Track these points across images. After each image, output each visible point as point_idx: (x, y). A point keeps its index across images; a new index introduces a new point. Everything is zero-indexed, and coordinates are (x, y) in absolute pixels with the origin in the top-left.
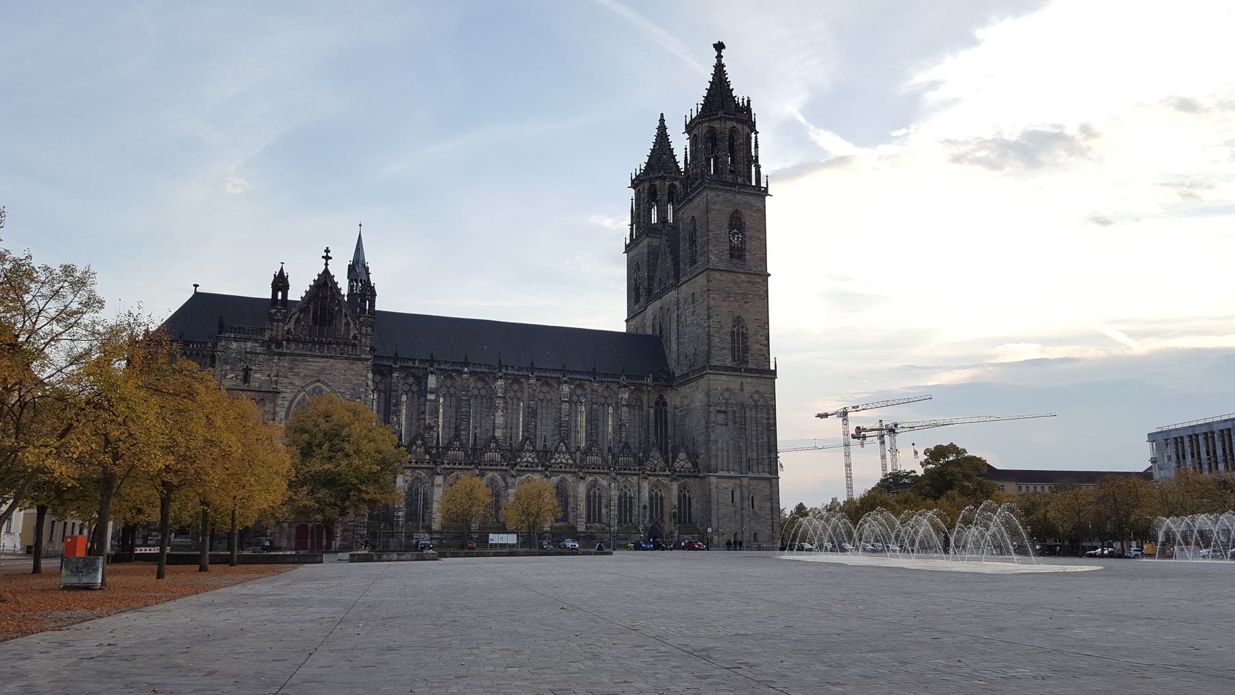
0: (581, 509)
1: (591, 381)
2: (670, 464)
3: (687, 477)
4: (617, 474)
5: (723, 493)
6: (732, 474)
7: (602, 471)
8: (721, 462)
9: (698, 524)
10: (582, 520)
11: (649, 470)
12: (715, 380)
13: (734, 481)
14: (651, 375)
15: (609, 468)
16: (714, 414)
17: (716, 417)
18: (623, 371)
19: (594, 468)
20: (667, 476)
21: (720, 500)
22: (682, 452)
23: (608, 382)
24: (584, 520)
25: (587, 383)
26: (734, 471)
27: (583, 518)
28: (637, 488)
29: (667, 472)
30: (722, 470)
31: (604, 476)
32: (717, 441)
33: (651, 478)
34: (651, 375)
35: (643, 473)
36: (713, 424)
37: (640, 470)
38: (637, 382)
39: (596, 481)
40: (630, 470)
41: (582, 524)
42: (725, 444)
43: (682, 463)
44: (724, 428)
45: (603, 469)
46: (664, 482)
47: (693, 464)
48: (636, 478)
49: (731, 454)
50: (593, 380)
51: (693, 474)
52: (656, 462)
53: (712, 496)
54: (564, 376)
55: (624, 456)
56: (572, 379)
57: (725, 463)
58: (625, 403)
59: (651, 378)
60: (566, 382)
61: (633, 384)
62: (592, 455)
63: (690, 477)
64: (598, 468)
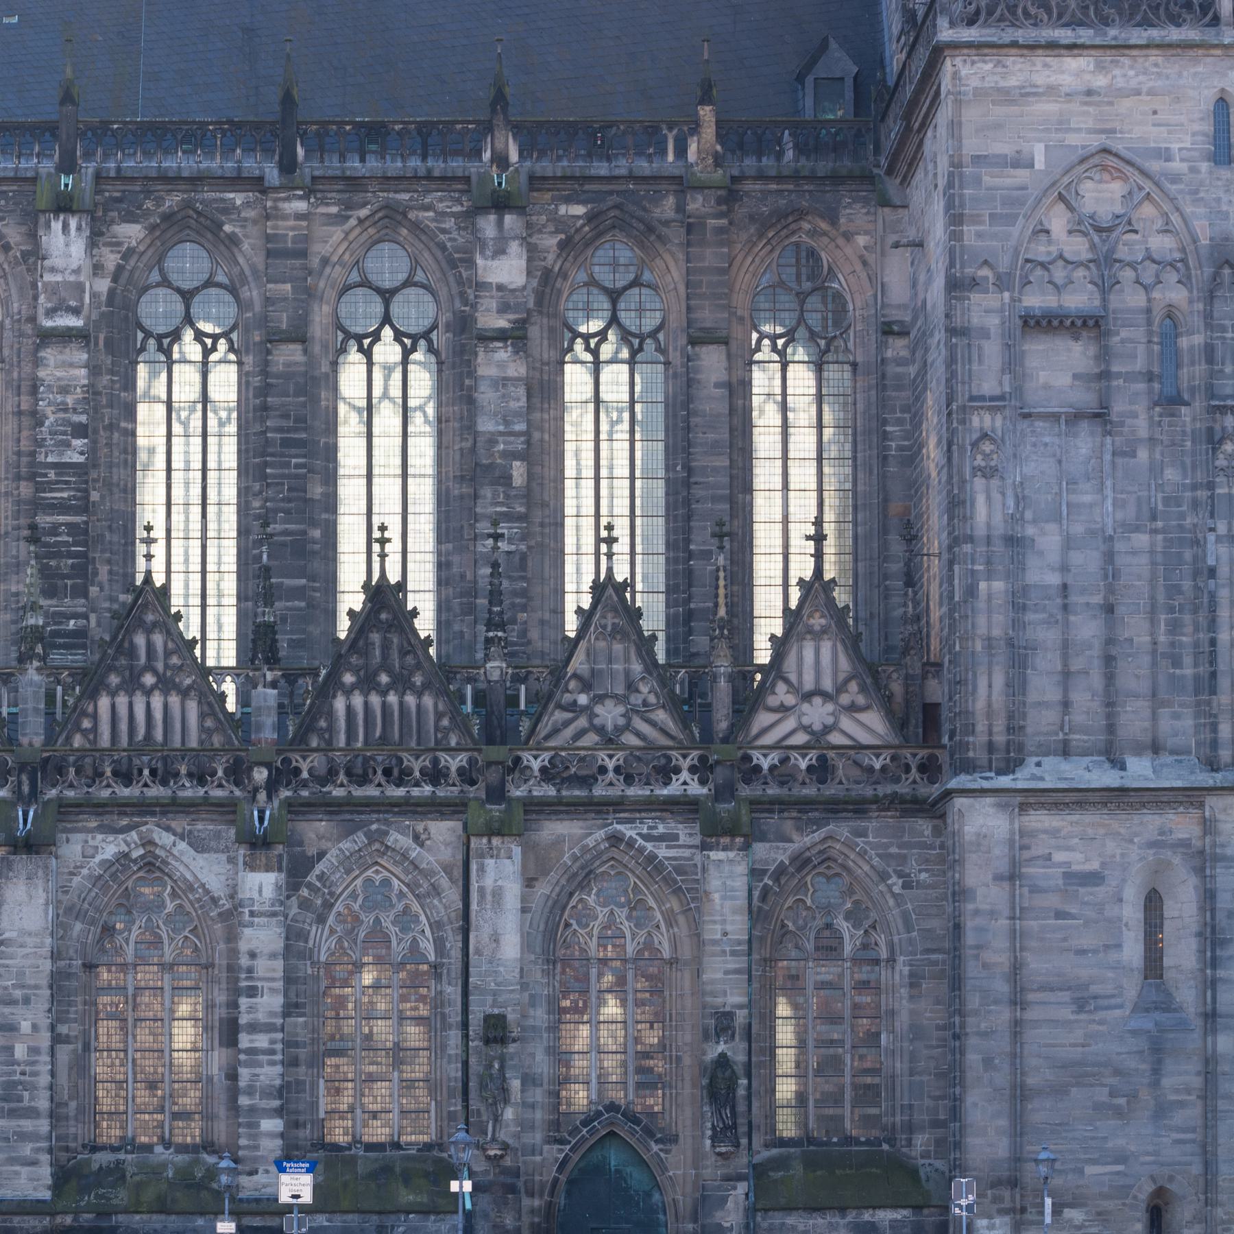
0: (20, 1051)
1: (257, 183)
2: (722, 725)
3: (835, 808)
4: (295, 808)
5: (1060, 915)
6: (1140, 771)
7: (190, 791)
8: (1053, 694)
9: (921, 1141)
10: (27, 1125)
11: (547, 774)
12: (1005, 96)
13: (1151, 822)
14: (706, 113)
15: (238, 772)
16: (992, 350)
17: (1013, 364)
18: (499, 100)
19: (125, 776)
20: (684, 807)
21: (1037, 965)
22: (818, 636)
23: (387, 181)
24: (44, 1126)
25: (238, 198)
26: (1156, 748)
27: (33, 1113)
28: (452, 894)
29: (686, 784)
30: (1065, 751)
31: (203, 827)
32: (1013, 541)
33: (555, 829)
34: (706, 113)
35: (497, 794)
36: (981, 421)
37: (467, 776)
38: (601, 168)
39: (153, 865)
40: (399, 776)
41: (27, 1150)
42: (1088, 561)
43: (817, 713)
44: (1084, 443)
45: (200, 778)
46: (663, 852)
47: (899, 723)
48: (443, 831)
49: (1136, 629)
50: (272, 174)
51: (886, 789)
52: (609, 714)
53: (970, 939)
54: (68, 165)
55: (367, 683)
56: (120, 177)
57: (1086, 701)
58: (502, 323)
59: (709, 131)
60: (64, 205)
61: (574, 186)
62: (132, 684)
63: (857, 808)
64: (164, 775)
